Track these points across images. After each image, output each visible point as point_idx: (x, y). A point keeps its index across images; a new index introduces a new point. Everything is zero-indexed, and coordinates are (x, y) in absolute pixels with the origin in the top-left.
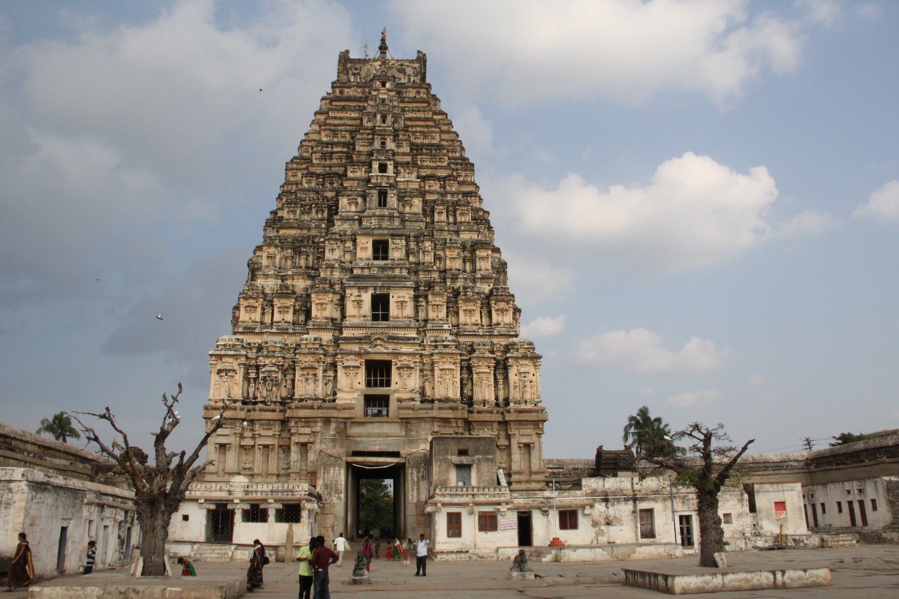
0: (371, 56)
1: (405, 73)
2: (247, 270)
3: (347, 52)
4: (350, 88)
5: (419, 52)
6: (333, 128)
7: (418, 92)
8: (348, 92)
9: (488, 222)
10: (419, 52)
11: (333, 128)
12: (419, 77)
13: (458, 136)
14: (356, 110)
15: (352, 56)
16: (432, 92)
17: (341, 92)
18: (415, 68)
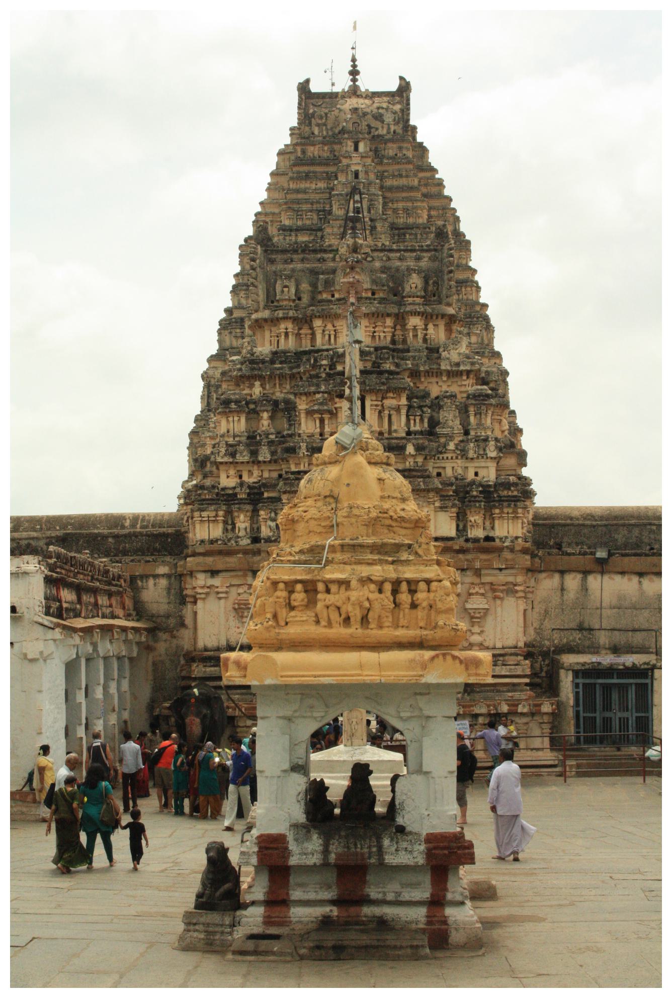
0: (337, 89)
1: (383, 122)
2: (201, 384)
3: (307, 81)
4: (314, 145)
5: (402, 78)
6: (295, 206)
7: (400, 148)
8: (313, 151)
9: (487, 319)
10: (401, 78)
11: (295, 206)
12: (401, 126)
13: (451, 200)
14: (324, 179)
15: (314, 88)
16: (419, 139)
17: (303, 152)
18: (395, 113)
